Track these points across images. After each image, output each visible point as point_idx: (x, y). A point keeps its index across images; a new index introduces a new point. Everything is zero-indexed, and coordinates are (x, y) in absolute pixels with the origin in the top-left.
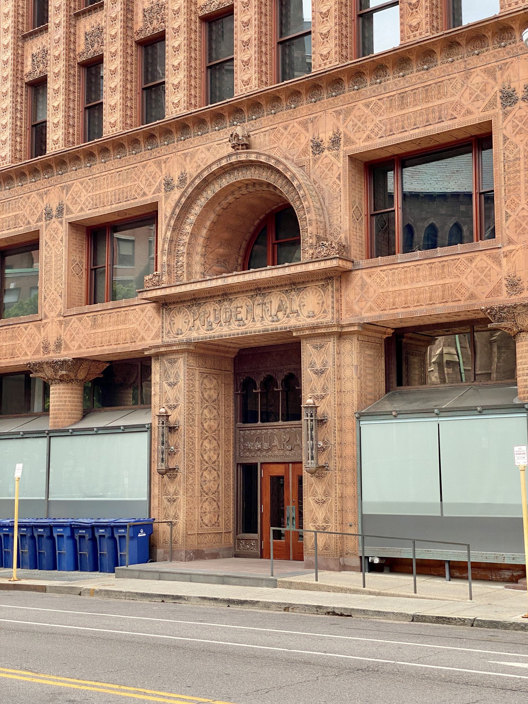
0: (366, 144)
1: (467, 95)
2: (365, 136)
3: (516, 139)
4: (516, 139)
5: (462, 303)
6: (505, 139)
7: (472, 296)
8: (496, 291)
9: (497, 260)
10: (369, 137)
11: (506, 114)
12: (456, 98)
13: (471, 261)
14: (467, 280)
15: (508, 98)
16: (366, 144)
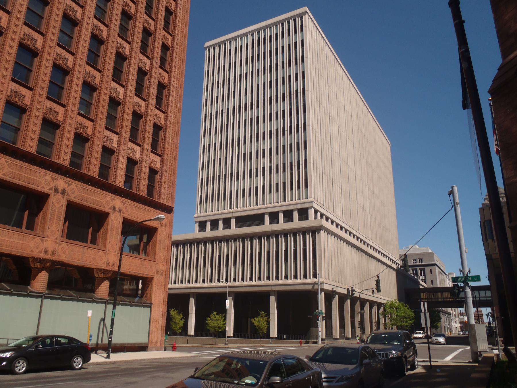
0: (2, 176)
1: (44, 181)
2: (3, 173)
3: (56, 205)
4: (56, 205)
5: (28, 252)
6: (53, 203)
7: (32, 251)
8: (40, 252)
9: (43, 241)
10: (4, 174)
11: (55, 195)
12: (40, 180)
13: (34, 238)
14: (32, 245)
15: (56, 190)
16: (2, 176)
